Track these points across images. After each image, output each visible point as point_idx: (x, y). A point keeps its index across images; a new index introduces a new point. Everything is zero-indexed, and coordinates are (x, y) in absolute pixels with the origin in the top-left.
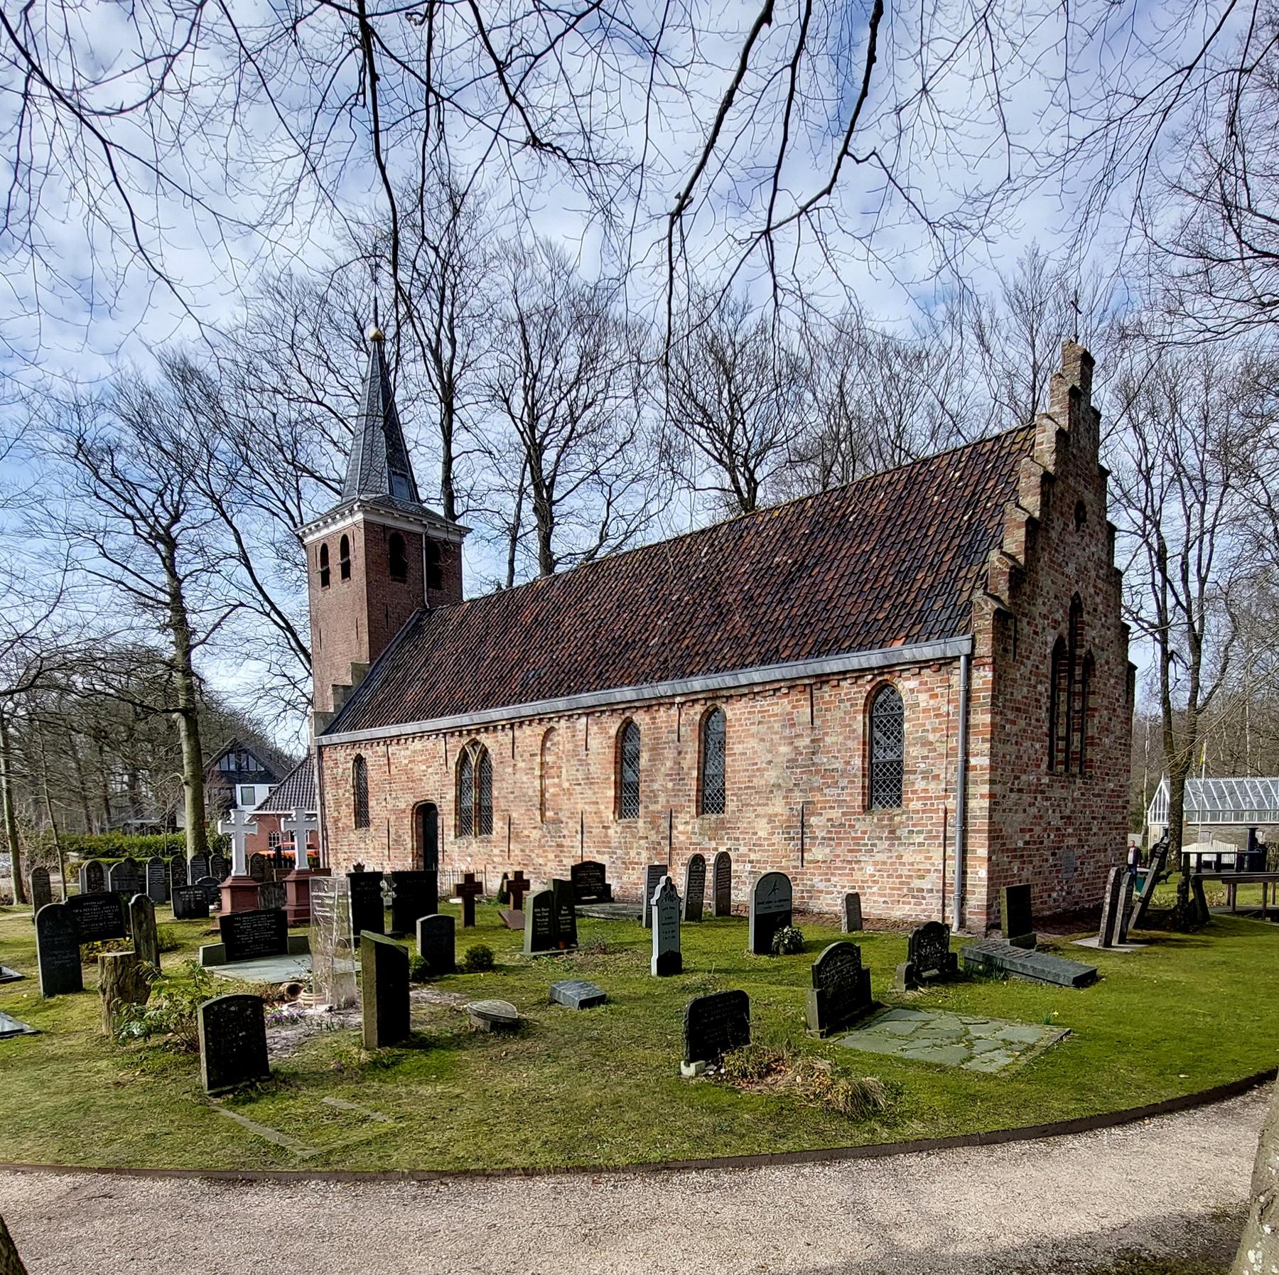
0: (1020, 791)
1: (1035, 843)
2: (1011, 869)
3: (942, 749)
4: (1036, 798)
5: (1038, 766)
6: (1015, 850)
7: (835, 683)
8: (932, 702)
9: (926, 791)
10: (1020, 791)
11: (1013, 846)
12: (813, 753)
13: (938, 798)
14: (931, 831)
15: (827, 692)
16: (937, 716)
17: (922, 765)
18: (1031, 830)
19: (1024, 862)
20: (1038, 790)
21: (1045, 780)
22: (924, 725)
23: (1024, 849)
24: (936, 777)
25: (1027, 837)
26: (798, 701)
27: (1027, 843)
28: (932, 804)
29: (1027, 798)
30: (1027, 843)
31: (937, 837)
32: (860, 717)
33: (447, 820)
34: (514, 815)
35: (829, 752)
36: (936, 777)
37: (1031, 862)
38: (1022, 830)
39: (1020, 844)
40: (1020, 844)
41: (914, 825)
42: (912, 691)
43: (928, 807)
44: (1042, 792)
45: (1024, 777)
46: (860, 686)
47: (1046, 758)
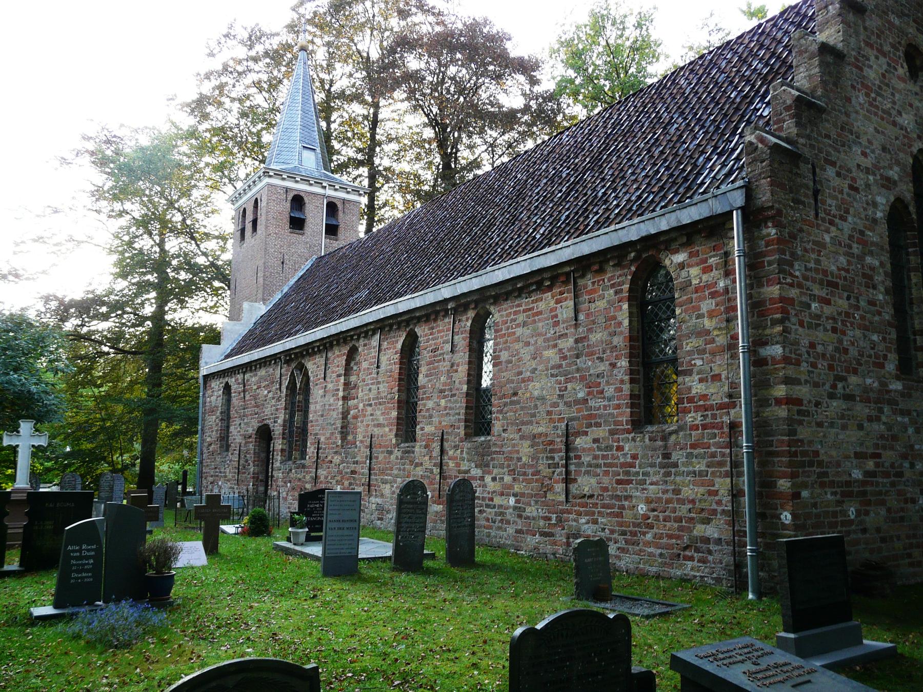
0: (849, 397)
1: (886, 475)
2: (844, 513)
3: (721, 340)
4: (881, 411)
5: (882, 366)
6: (848, 484)
7: (596, 267)
8: (705, 277)
9: (704, 397)
10: (849, 397)
11: (845, 478)
12: (578, 356)
13: (721, 407)
14: (713, 455)
15: (588, 282)
16: (713, 295)
17: (699, 362)
18: (878, 456)
19: (868, 503)
20: (882, 398)
21: (897, 386)
22: (699, 308)
23: (864, 483)
24: (716, 378)
25: (870, 465)
26: (561, 293)
27: (867, 474)
28: (714, 416)
29: (862, 410)
30: (867, 474)
31: (721, 464)
32: (625, 306)
33: (278, 444)
34: (322, 439)
35: (592, 354)
36: (716, 378)
37: (883, 503)
38: (858, 455)
39: (857, 474)
40: (857, 474)
41: (693, 446)
42: (682, 266)
43: (709, 420)
44: (892, 402)
45: (853, 379)
46: (623, 267)
47: (893, 357)
